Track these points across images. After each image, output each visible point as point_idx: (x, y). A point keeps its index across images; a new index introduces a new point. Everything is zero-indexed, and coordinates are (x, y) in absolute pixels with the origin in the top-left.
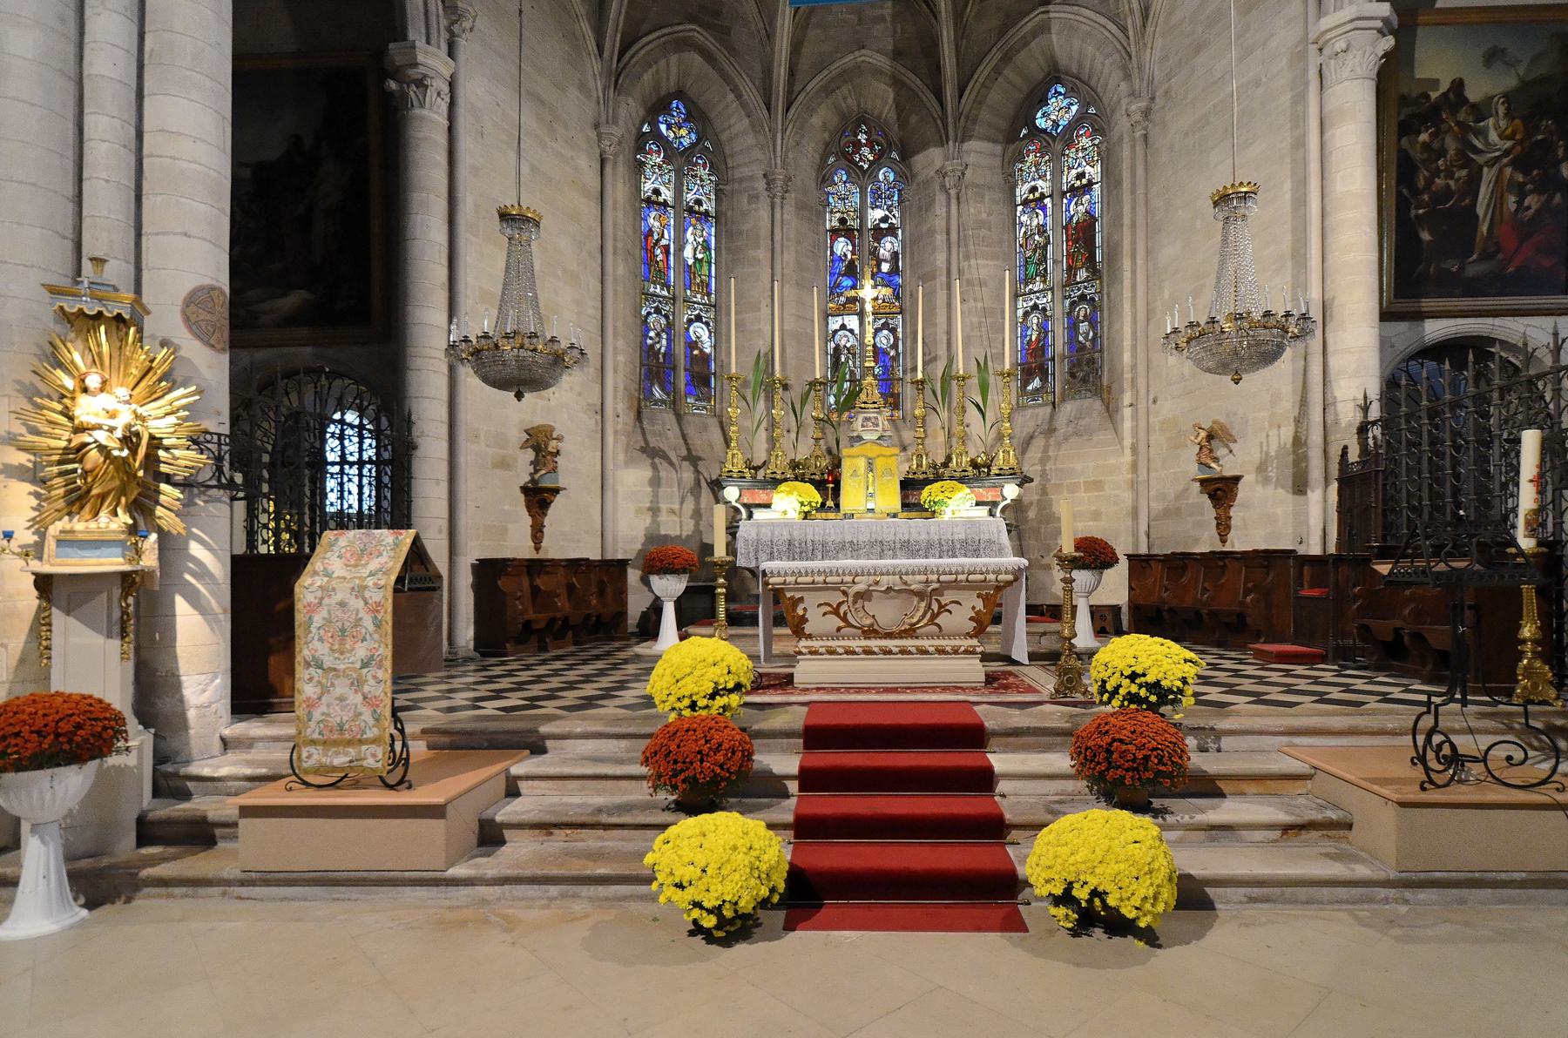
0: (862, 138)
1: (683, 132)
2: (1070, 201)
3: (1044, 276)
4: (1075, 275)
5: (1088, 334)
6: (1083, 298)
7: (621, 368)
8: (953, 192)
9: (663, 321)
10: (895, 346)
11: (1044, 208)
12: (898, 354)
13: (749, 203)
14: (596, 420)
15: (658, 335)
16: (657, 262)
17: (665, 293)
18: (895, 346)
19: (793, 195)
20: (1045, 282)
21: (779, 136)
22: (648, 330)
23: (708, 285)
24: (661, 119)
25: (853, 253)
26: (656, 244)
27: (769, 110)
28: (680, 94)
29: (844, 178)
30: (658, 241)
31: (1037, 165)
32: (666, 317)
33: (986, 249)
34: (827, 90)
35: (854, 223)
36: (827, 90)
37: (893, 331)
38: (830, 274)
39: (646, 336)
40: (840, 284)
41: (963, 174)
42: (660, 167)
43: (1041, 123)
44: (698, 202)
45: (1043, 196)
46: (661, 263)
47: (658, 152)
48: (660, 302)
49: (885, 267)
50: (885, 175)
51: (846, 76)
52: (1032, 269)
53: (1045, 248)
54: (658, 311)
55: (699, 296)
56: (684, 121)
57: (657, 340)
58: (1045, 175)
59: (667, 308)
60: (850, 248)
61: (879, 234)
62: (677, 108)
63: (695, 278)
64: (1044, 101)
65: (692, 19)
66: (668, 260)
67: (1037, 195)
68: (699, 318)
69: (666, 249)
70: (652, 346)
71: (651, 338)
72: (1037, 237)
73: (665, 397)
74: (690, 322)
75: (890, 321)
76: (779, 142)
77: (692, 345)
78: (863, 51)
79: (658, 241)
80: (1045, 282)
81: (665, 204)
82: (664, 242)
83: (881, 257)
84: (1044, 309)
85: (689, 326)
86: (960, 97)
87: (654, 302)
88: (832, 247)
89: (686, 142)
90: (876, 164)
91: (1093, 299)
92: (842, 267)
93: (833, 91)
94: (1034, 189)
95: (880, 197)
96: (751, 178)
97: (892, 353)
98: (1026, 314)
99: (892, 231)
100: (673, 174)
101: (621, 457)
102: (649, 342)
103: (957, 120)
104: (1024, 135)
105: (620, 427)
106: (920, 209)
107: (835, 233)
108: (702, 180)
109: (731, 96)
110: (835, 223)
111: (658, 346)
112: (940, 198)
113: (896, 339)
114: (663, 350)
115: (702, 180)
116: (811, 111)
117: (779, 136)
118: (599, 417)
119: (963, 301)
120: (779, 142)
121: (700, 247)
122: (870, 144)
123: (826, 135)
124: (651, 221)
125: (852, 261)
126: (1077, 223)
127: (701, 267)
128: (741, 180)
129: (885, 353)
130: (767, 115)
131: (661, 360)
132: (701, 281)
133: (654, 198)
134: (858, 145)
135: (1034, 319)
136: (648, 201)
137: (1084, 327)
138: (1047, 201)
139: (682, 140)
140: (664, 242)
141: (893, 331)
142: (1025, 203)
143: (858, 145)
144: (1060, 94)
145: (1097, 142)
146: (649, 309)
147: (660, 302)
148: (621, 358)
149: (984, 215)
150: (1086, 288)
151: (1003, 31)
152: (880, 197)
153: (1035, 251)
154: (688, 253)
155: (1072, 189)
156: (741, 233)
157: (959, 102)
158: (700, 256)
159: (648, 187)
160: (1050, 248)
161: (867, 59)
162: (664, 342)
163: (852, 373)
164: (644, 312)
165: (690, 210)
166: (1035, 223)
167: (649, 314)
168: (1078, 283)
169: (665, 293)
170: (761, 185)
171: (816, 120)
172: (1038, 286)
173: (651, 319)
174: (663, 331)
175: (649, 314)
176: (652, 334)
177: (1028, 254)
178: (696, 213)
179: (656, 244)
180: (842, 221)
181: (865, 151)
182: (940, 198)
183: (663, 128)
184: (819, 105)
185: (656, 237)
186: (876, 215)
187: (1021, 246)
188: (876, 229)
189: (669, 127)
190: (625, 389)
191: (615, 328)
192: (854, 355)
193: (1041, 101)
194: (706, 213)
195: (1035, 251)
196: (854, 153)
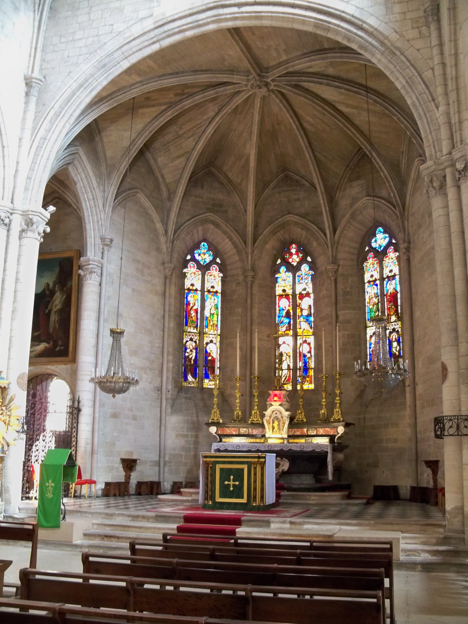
0: (293, 251)
1: (207, 255)
2: (387, 282)
4: (390, 318)
5: (396, 347)
6: (394, 330)
7: (171, 369)
9: (194, 344)
10: (310, 352)
12: (311, 356)
13: (236, 286)
14: (158, 394)
15: (191, 351)
16: (192, 317)
17: (195, 331)
18: (310, 352)
19: (257, 282)
21: (250, 256)
22: (186, 349)
23: (217, 326)
24: (195, 252)
25: (289, 306)
26: (191, 309)
27: (245, 244)
28: (205, 240)
29: (285, 270)
30: (192, 307)
31: (373, 264)
32: (195, 342)
33: (349, 305)
34: (273, 233)
35: (289, 292)
36: (273, 233)
37: (309, 344)
38: (278, 317)
39: (185, 351)
40: (282, 322)
41: (338, 270)
42: (195, 273)
43: (374, 245)
44: (213, 287)
45: (376, 280)
46: (194, 318)
47: (194, 267)
48: (192, 335)
49: (305, 313)
50: (305, 268)
51: (282, 226)
54: (191, 340)
55: (212, 331)
56: (207, 251)
57: (191, 353)
58: (377, 270)
59: (196, 338)
60: (288, 303)
61: (302, 297)
62: (204, 246)
63: (210, 323)
64: (374, 235)
65: (209, 210)
66: (197, 315)
67: (374, 279)
68: (211, 341)
69: (196, 311)
70: (188, 356)
71: (188, 353)
73: (194, 380)
74: (207, 344)
75: (307, 339)
76: (250, 258)
77: (207, 354)
78: (290, 215)
79: (192, 307)
81: (196, 290)
82: (195, 308)
83: (303, 308)
85: (207, 346)
86: (334, 234)
87: (190, 335)
88: (279, 303)
89: (208, 261)
90: (300, 264)
91: (398, 331)
92: (284, 313)
93: (276, 233)
94: (372, 276)
95: (302, 279)
96: (238, 275)
97: (309, 355)
98: (371, 337)
99: (308, 295)
100: (200, 276)
101: (169, 410)
102: (187, 354)
104: (368, 250)
105: (169, 396)
106: (320, 285)
107: (281, 296)
108: (215, 277)
109: (227, 240)
110: (281, 293)
111: (191, 356)
113: (310, 348)
114: (193, 358)
115: (215, 277)
116: (266, 242)
117: (250, 256)
118: (159, 392)
119: (339, 331)
120: (250, 258)
121: (213, 308)
122: (297, 254)
123: (275, 252)
124: (189, 299)
125: (288, 310)
126: (390, 293)
127: (213, 317)
128: (233, 276)
129: (305, 356)
130: (244, 246)
131: (192, 362)
132: (213, 324)
133: (191, 288)
134: (291, 254)
136: (189, 289)
137: (395, 344)
139: (205, 260)
140: (194, 308)
141: (309, 344)
142: (369, 282)
143: (291, 254)
144: (381, 232)
145: (396, 256)
146: (187, 339)
147: (192, 335)
148: (171, 365)
149: (348, 289)
150: (395, 325)
151: (352, 205)
152: (302, 279)
153: (373, 305)
154: (207, 313)
155: (388, 277)
156: (232, 300)
157: (334, 237)
158: (212, 312)
159: (187, 284)
160: (380, 304)
161: (291, 218)
162: (194, 354)
163: (289, 366)
164: (184, 341)
165: (209, 291)
167: (187, 341)
168: (392, 323)
169: (195, 331)
170: (241, 278)
171: (268, 246)
173: (188, 344)
174: (193, 349)
175: (187, 341)
176: (188, 351)
177: (371, 307)
178: (211, 292)
179: (191, 309)
180: (284, 291)
181: (295, 257)
183: (196, 256)
184: (270, 239)
185: (191, 305)
186: (299, 289)
187: (368, 303)
188: (301, 294)
189: (199, 255)
190: (173, 378)
191: (168, 351)
192: (289, 356)
193: (373, 235)
194: (216, 292)
195: (373, 305)
196: (289, 258)
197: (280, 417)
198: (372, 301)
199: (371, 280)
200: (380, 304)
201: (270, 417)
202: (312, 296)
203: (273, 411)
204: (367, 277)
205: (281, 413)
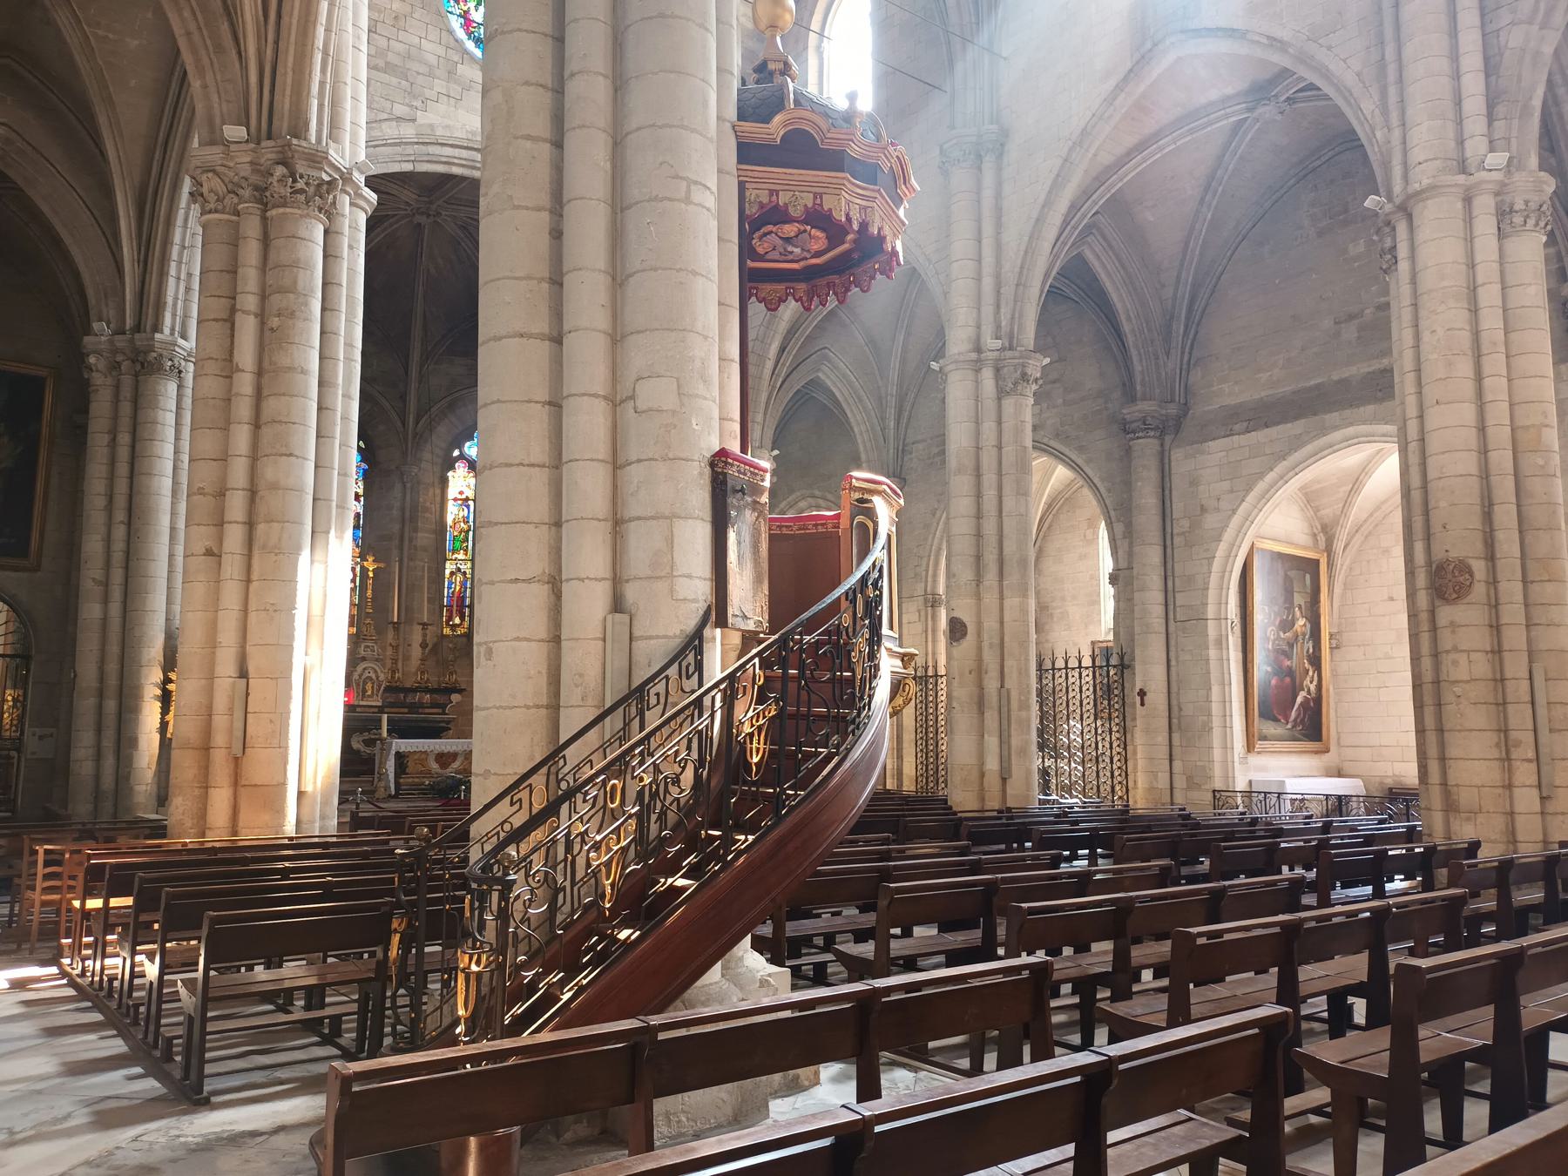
3: (466, 551)
8: (408, 485)
11: (468, 507)
20: (466, 555)
45: (467, 499)
52: (458, 544)
53: (467, 532)
72: (462, 524)
80: (466, 555)
84: (465, 573)
86: (417, 423)
98: (452, 574)
103: (414, 437)
112: (398, 487)
135: (459, 577)
138: (471, 503)
142: (455, 500)
153: (461, 532)
160: (471, 533)
166: (461, 515)
172: (461, 556)
177: (456, 534)
182: (398, 487)
195: (461, 532)
197: (374, 677)
198: (457, 525)
199: (459, 497)
200: (471, 533)
201: (360, 676)
202: (362, 499)
203: (365, 669)
204: (452, 492)
205: (376, 672)
